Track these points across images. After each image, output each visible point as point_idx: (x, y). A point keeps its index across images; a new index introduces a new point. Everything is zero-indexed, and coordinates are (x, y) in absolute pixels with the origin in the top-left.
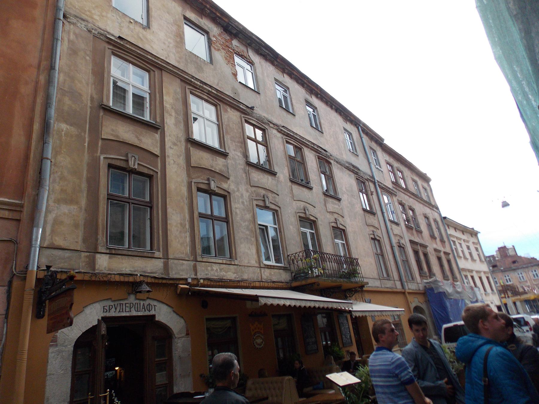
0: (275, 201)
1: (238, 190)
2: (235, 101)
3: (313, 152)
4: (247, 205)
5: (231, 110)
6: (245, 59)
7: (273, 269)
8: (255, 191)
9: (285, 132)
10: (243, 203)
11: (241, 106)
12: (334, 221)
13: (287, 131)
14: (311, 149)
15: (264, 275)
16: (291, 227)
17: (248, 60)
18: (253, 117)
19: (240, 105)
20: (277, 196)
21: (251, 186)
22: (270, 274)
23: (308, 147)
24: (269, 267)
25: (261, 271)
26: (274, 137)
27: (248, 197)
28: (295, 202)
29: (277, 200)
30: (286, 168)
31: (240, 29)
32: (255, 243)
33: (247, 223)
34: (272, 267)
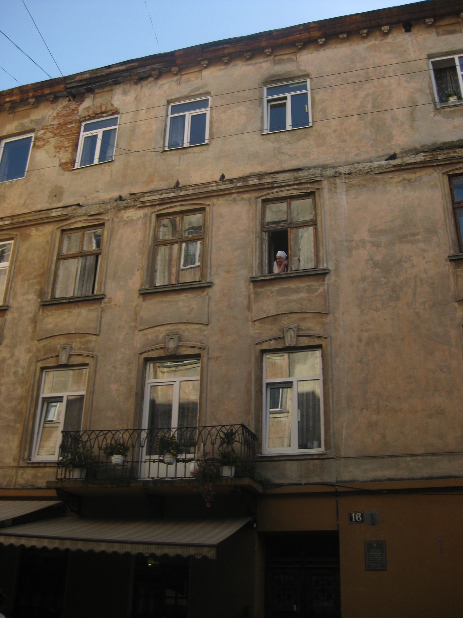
0: (87, 349)
1: (12, 355)
2: (43, 212)
3: (246, 196)
4: (23, 375)
5: (37, 230)
6: (105, 115)
7: (45, 467)
8: (44, 346)
9: (152, 201)
10: (16, 373)
11: (54, 214)
12: (279, 334)
13: (159, 197)
14: (238, 193)
15: (22, 478)
16: (114, 387)
17: (110, 113)
18: (78, 217)
19: (52, 212)
20: (94, 338)
21: (38, 340)
22: (35, 476)
23: (231, 194)
24: (36, 465)
25: (17, 472)
26: (124, 224)
27: (27, 361)
28: (141, 333)
29: (91, 345)
30: (138, 273)
31: (86, 79)
32: (20, 431)
33: (14, 403)
34: (41, 465)
